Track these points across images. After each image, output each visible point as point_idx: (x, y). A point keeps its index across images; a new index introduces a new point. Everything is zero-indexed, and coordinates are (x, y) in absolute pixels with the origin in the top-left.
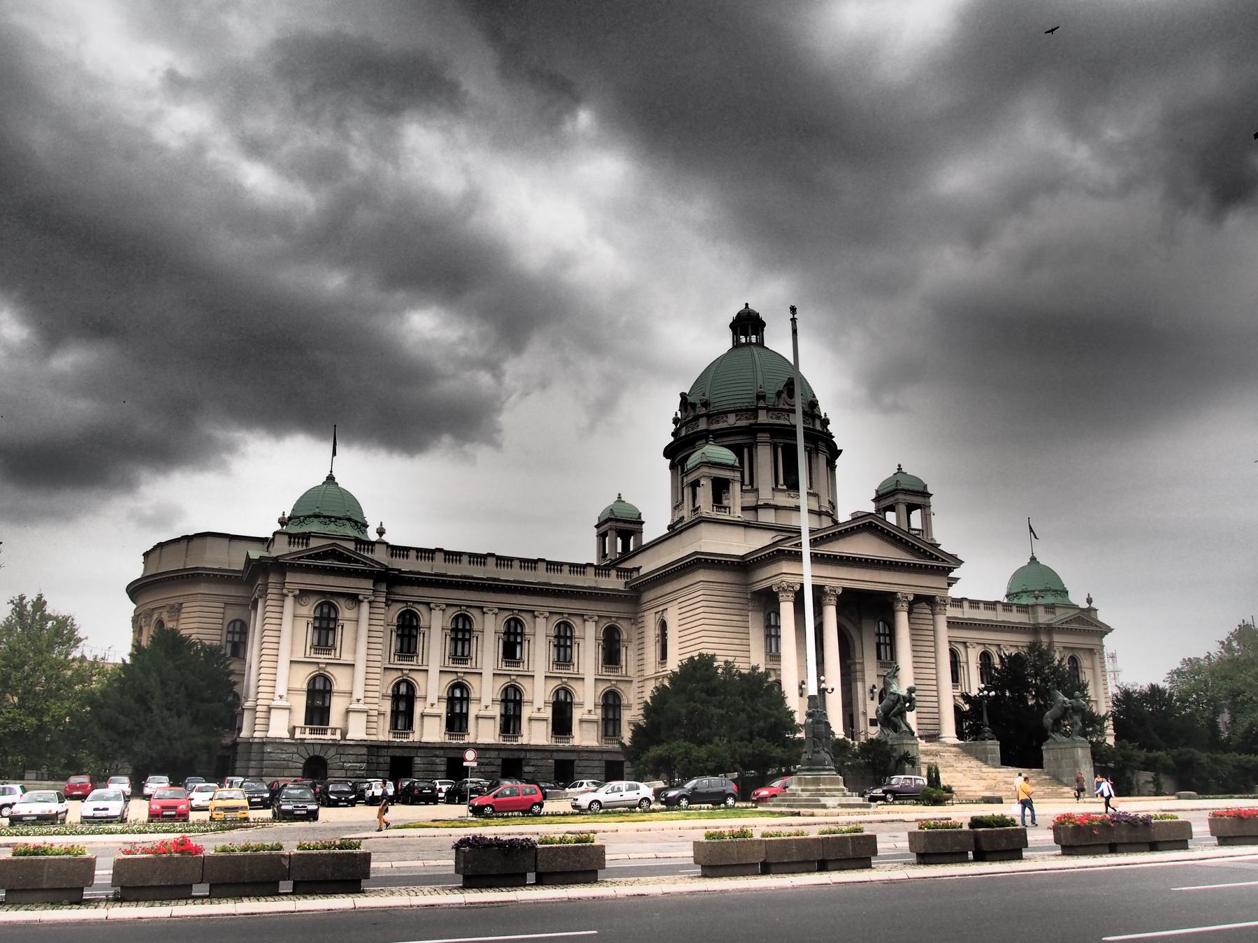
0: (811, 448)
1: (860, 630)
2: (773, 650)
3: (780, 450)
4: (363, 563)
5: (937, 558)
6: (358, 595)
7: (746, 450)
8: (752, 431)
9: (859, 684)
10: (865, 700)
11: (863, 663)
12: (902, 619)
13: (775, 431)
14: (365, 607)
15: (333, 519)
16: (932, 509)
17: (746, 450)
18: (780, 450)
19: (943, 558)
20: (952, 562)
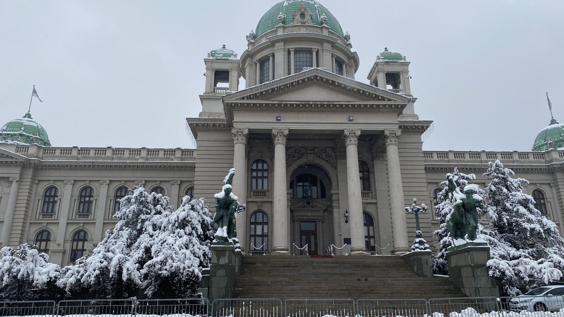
0: (318, 49)
1: (336, 168)
2: (254, 187)
3: (292, 53)
4: (11, 157)
5: (383, 99)
6: (9, 177)
7: (271, 58)
8: (272, 44)
9: (335, 211)
10: (340, 223)
11: (338, 194)
12: (352, 152)
13: (286, 41)
14: (14, 186)
15: (10, 136)
16: (410, 74)
17: (271, 58)
18: (292, 53)
19: (389, 97)
20: (399, 101)
